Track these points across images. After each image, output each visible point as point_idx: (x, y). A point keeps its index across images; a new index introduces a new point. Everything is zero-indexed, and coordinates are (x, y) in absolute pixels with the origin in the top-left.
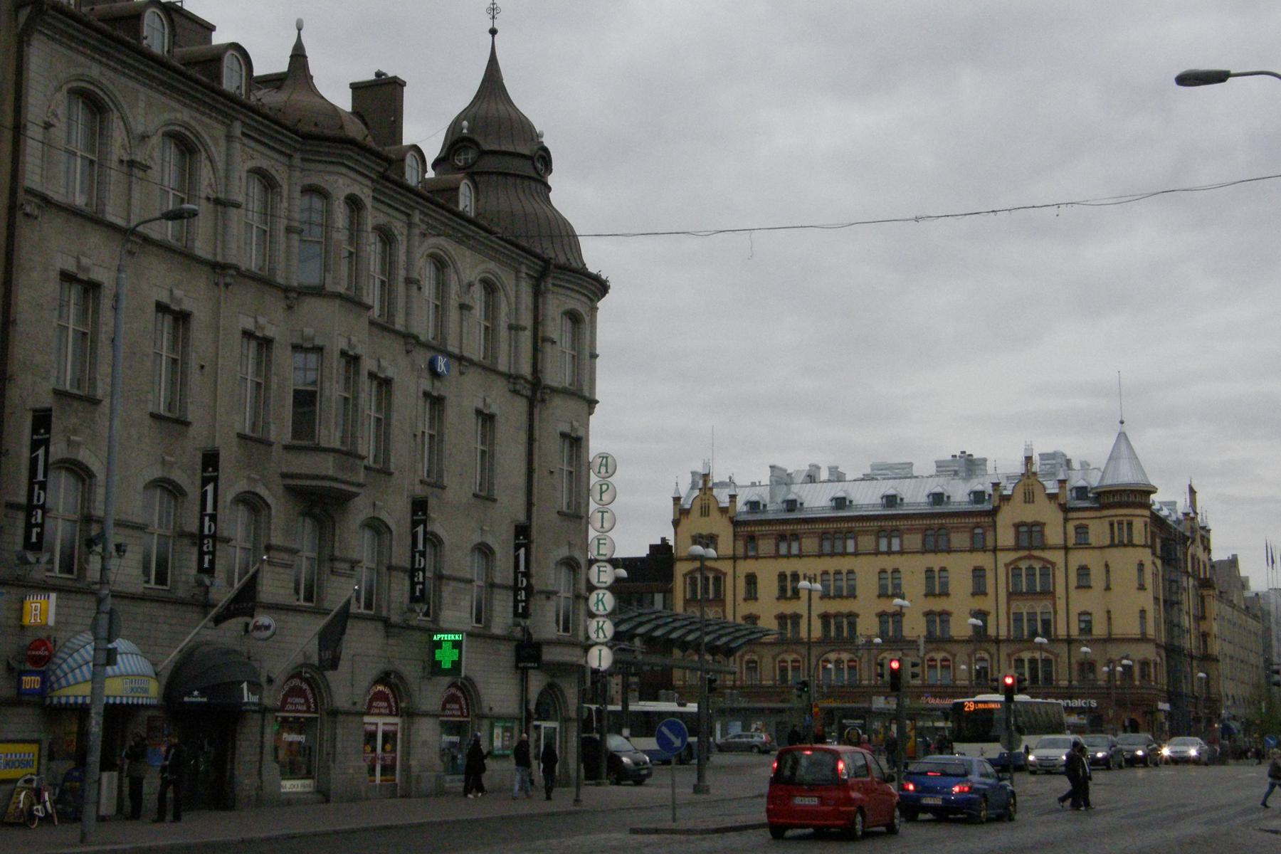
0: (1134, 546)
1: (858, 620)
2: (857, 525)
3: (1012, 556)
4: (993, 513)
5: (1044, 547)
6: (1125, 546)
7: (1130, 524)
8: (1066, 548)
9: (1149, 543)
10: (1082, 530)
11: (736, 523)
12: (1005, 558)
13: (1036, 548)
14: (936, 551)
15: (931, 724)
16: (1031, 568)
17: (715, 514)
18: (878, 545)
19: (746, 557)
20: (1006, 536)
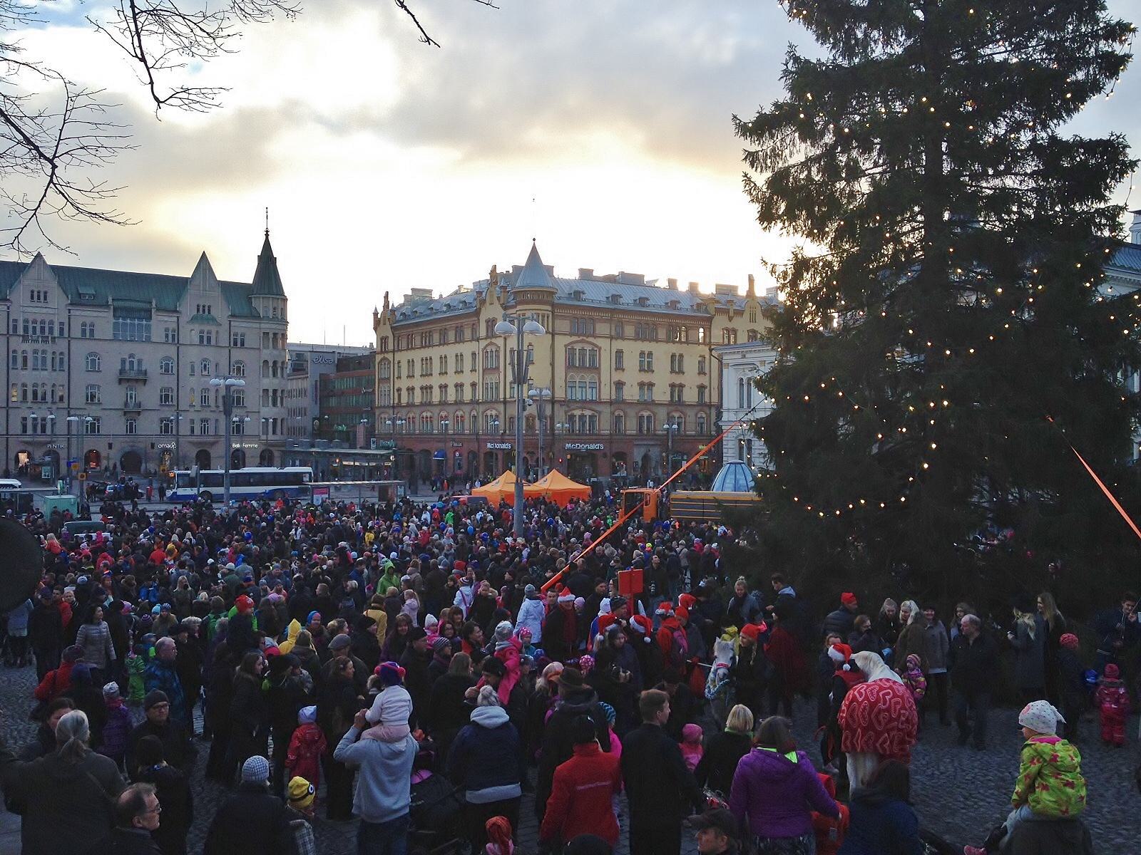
1: (448, 389)
2: (595, 315)
4: (477, 313)
9: (551, 330)
12: (483, 343)
15: (352, 463)
16: (492, 351)
19: (399, 350)
20: (482, 332)
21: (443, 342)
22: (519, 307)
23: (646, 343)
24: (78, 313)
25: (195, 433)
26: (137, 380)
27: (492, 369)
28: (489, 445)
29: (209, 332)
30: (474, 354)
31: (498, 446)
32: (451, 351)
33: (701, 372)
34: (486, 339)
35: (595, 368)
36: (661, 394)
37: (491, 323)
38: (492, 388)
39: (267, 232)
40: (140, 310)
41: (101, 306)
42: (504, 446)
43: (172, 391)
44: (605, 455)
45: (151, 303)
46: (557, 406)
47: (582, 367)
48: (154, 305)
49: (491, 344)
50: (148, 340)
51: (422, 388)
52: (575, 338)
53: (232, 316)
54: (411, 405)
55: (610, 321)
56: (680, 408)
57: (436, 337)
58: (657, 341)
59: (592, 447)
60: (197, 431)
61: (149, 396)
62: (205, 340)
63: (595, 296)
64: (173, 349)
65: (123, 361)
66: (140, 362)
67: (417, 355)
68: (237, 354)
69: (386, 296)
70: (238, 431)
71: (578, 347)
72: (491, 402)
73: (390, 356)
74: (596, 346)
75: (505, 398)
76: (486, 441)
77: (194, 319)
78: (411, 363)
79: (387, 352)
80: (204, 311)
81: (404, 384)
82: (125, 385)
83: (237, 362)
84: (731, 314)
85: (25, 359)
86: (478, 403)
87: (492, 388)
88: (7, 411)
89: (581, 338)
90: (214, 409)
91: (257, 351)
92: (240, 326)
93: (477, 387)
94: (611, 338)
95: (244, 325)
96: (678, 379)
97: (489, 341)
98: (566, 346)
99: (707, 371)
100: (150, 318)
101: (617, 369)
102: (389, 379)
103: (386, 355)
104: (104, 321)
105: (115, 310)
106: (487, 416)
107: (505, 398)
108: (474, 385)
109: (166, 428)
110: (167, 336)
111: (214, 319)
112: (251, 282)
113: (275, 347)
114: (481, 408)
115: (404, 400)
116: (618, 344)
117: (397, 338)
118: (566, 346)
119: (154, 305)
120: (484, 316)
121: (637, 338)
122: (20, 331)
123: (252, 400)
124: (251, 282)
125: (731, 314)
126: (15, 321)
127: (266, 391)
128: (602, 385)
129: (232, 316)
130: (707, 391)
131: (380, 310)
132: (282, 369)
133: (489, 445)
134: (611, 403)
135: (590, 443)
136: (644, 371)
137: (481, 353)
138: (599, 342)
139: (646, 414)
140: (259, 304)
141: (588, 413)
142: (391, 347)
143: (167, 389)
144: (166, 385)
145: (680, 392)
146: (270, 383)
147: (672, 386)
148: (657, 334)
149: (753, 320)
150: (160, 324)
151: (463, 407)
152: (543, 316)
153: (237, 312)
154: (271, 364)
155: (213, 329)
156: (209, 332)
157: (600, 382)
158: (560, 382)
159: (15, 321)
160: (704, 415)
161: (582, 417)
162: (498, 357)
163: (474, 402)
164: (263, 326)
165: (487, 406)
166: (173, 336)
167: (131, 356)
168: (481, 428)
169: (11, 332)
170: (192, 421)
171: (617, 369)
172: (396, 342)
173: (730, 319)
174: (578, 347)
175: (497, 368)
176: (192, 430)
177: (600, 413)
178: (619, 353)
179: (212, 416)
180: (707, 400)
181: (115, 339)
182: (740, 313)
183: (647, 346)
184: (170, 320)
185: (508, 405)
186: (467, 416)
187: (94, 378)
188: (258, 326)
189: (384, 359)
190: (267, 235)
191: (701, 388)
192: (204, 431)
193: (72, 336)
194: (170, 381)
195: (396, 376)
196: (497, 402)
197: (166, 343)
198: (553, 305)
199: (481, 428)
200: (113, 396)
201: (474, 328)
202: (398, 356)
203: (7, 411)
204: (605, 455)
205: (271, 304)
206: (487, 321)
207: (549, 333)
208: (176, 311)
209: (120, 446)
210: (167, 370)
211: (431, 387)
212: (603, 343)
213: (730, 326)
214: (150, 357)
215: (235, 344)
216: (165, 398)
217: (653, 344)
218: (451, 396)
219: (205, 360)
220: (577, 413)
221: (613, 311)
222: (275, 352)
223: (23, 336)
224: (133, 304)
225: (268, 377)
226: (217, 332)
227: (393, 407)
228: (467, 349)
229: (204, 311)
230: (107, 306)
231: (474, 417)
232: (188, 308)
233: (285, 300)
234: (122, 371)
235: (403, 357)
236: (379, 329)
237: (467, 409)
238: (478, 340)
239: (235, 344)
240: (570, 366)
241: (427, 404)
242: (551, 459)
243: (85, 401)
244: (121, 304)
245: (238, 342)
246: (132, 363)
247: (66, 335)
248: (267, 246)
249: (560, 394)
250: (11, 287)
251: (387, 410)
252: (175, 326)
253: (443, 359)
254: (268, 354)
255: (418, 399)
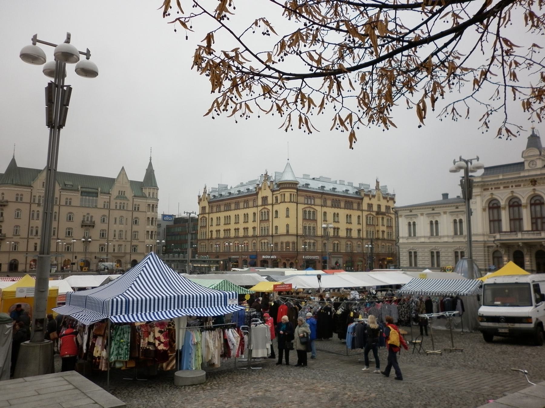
0: (286, 202)
3: (261, 208)
4: (257, 194)
5: (267, 205)
6: (283, 202)
7: (284, 195)
8: (273, 205)
10: (276, 198)
11: (209, 203)
12: (260, 208)
13: (265, 205)
14: (335, 207)
15: (199, 265)
16: (265, 212)
17: (206, 200)
18: (244, 206)
19: (212, 213)
20: (260, 202)
21: (237, 208)
22: (281, 191)
23: (336, 209)
24: (64, 193)
25: (115, 252)
26: (90, 226)
27: (265, 220)
28: (263, 257)
29: (124, 203)
30: (254, 214)
31: (269, 257)
32: (241, 213)
33: (359, 223)
34: (262, 206)
35: (315, 220)
36: (343, 233)
37: (265, 199)
38: (265, 230)
39: (151, 158)
40: (93, 193)
41: (75, 190)
42: (272, 257)
43: (106, 231)
44: (319, 262)
45: (98, 189)
46: (299, 237)
47: (309, 219)
48: (99, 191)
49: (265, 208)
50: (96, 207)
51: (224, 230)
52: (306, 206)
53: (135, 196)
54: (218, 239)
55: (321, 198)
56: (350, 240)
57: (233, 206)
58: (340, 208)
59: (314, 257)
60: (116, 251)
61: (95, 233)
62: (122, 208)
63: (315, 186)
64: (108, 211)
65: (84, 216)
66: (92, 217)
67: (222, 215)
68: (136, 214)
69: (205, 188)
70: (135, 251)
71: (308, 210)
72: (264, 236)
73: (207, 216)
74: (316, 210)
75: (272, 234)
76: (262, 255)
77: (117, 197)
78: (218, 219)
79: (205, 214)
80: (122, 194)
81: (214, 228)
82: (84, 228)
83: (136, 218)
84: (371, 196)
85: (38, 215)
86: (257, 237)
87: (265, 230)
88: (28, 240)
89: (309, 206)
90: (124, 240)
91: (144, 213)
92: (138, 201)
93: (256, 229)
94: (322, 206)
95: (139, 200)
96: (349, 226)
97: (263, 207)
98: (303, 209)
99: (361, 223)
100: (97, 196)
101: (324, 221)
102: (206, 226)
103: (205, 215)
104: (76, 198)
105: (82, 192)
106: (262, 243)
107: (272, 234)
108: (254, 228)
109: (102, 248)
110: (104, 205)
111: (126, 198)
112: (142, 181)
113: (153, 211)
114: (259, 239)
115: (214, 235)
116: (325, 209)
117: (211, 207)
118: (303, 209)
119: (99, 191)
120: (260, 196)
121: (333, 206)
122: (37, 202)
123: (142, 236)
124: (142, 181)
125: (371, 196)
126: (35, 196)
127: (148, 232)
128: (318, 228)
129: (135, 196)
130: (361, 232)
131: (202, 194)
132: (155, 221)
133: (263, 257)
134: (322, 237)
135: (313, 256)
136: (336, 222)
137: (259, 213)
138: (316, 208)
139: (336, 242)
140: (146, 191)
141: (312, 241)
142: (207, 211)
143: (103, 230)
144: (104, 229)
145: (350, 232)
146: (150, 228)
147: (347, 229)
148: (340, 205)
149: (379, 200)
150: (102, 200)
151: (249, 239)
152: (293, 195)
153: (136, 195)
154: (151, 219)
155: (126, 202)
156: (124, 203)
157: (317, 227)
158: (300, 227)
159: (35, 196)
160: (360, 243)
161: (309, 243)
162: (268, 214)
163: (254, 237)
164: (148, 201)
165: (261, 238)
166: (107, 205)
167: (88, 214)
168: (258, 248)
169: (32, 202)
170: (114, 246)
171: (324, 221)
172: (210, 209)
173: (370, 199)
174: (308, 210)
175: (268, 220)
176: (114, 251)
177: (317, 241)
178: (325, 213)
179: (123, 243)
180: (361, 236)
181: (81, 207)
182: (374, 196)
183: (336, 210)
184: (106, 197)
185: (274, 238)
186: (250, 243)
187: (70, 225)
188: (145, 201)
189: (204, 217)
190: (151, 160)
191: (359, 231)
192: (119, 249)
193: (61, 204)
194: (104, 226)
195: (210, 224)
196: (268, 236)
197: (104, 208)
198: (298, 190)
199: (258, 248)
200: (79, 233)
201: (255, 200)
202: (211, 215)
203: (28, 240)
204: (319, 262)
205: (152, 191)
206: (263, 198)
207: (295, 202)
208: (109, 194)
209: (80, 257)
210: (104, 221)
211: (230, 230)
212: (318, 208)
213: (370, 202)
214: (97, 215)
215: (135, 209)
216: (102, 235)
217: (339, 209)
218: (241, 233)
219: (122, 216)
220: (308, 241)
221: (323, 194)
222: (153, 213)
223: (38, 204)
224: (90, 190)
225: (149, 225)
226: (127, 204)
227: (208, 240)
228: (250, 211)
229: (122, 194)
230: (78, 190)
231: (254, 243)
232: (115, 192)
233: (158, 189)
234: (83, 221)
235: (214, 216)
236: (200, 203)
237: (250, 240)
238: (257, 206)
239: (135, 209)
240: (304, 219)
241: (227, 238)
242: (296, 263)
243: (65, 236)
244: (84, 189)
245: (136, 209)
246: (88, 218)
247: (58, 203)
248: (150, 164)
249: (300, 232)
250: (33, 180)
251: (204, 241)
252: (108, 200)
253: (237, 217)
254: (150, 214)
255: (222, 235)
